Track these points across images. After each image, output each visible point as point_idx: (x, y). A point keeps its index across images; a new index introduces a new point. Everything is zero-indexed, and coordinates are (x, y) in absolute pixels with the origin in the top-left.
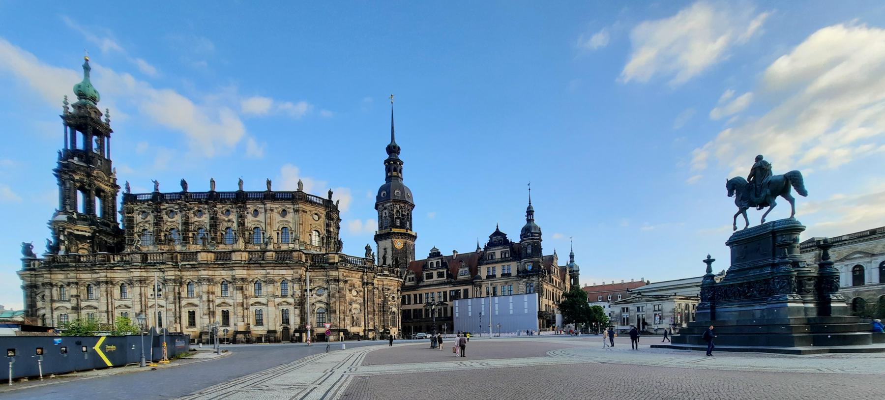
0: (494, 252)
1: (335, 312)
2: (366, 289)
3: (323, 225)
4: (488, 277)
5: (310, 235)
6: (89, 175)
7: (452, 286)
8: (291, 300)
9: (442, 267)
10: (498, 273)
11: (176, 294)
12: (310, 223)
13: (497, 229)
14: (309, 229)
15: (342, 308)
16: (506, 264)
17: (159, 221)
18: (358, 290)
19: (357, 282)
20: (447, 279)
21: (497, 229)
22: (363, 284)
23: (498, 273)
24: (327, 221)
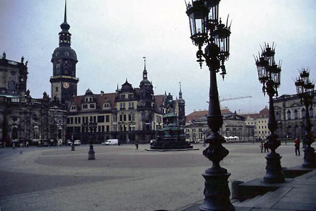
1: (24, 130)
3: (17, 78)
4: (121, 109)
9: (94, 102)
10: (127, 107)
13: (127, 82)
15: (28, 128)
16: (131, 102)
19: (38, 113)
21: (127, 82)
23: (127, 107)
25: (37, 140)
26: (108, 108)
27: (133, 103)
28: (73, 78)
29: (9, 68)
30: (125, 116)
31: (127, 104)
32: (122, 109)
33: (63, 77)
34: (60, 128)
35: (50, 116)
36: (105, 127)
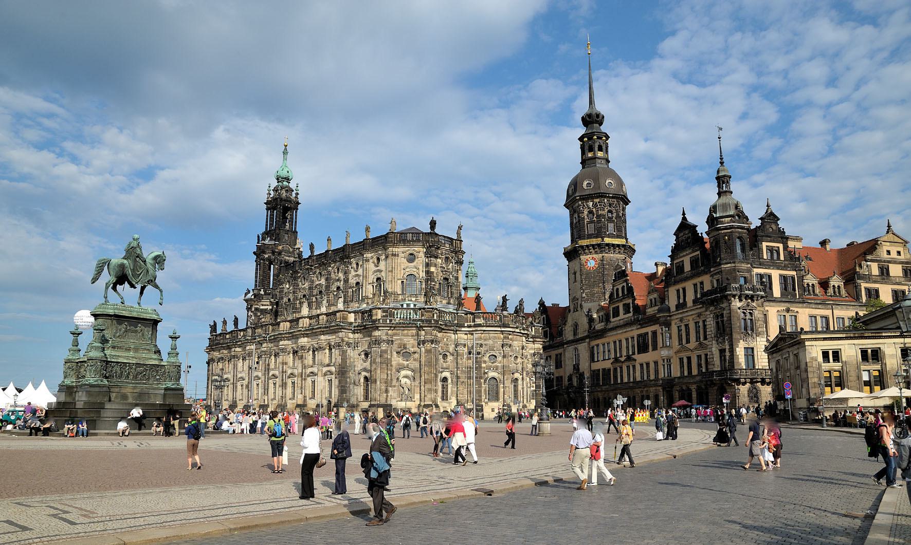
0: (683, 260)
2: (423, 349)
3: (421, 267)
4: (680, 306)
5: (402, 282)
6: (273, 253)
7: (639, 326)
8: (333, 369)
9: (628, 297)
10: (690, 297)
11: (267, 365)
12: (403, 267)
13: (684, 219)
14: (402, 275)
16: (697, 280)
17: (297, 289)
18: (410, 352)
20: (634, 315)
21: (684, 219)
22: (419, 344)
23: (690, 297)
24: (427, 260)
25: (409, 404)
26: (657, 308)
27: (702, 283)
28: (607, 240)
29: (401, 250)
30: (687, 326)
31: (689, 286)
32: (681, 306)
33: (584, 242)
34: (492, 374)
35: (465, 345)
36: (652, 366)
